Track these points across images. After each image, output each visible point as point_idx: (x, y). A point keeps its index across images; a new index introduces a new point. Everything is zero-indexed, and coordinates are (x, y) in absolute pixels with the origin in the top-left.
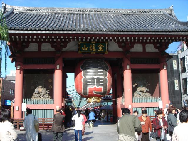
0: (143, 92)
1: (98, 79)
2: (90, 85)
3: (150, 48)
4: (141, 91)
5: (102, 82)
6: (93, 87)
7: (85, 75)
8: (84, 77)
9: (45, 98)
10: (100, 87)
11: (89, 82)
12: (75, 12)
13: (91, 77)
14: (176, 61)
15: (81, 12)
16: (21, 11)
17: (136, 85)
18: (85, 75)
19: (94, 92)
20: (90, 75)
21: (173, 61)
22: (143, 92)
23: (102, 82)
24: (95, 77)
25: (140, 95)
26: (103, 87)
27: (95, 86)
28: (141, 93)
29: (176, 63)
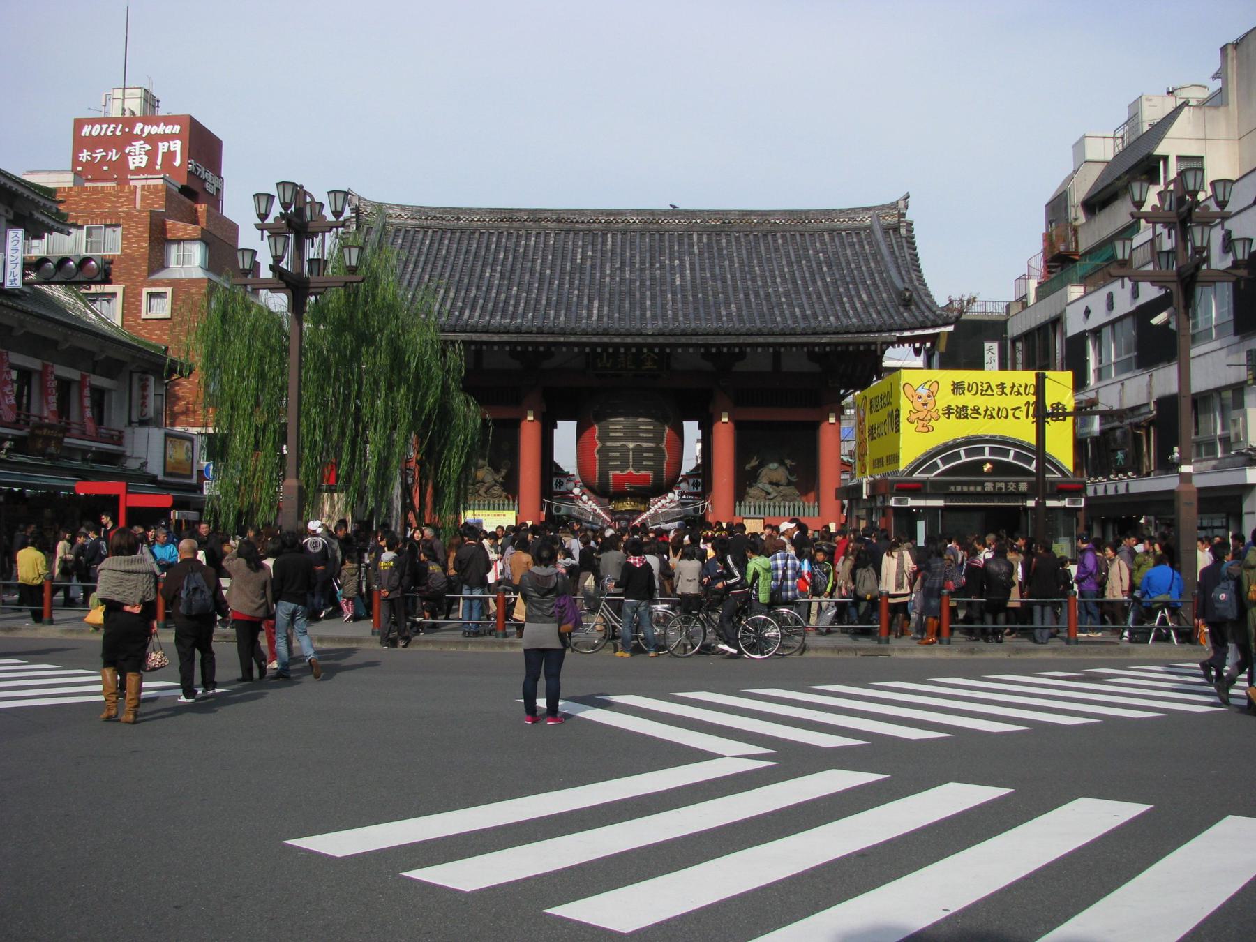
0: (777, 484)
1: (638, 450)
2: (616, 468)
3: (795, 364)
4: (771, 483)
5: (648, 459)
6: (625, 473)
7: (604, 437)
8: (599, 445)
9: (493, 496)
10: (644, 472)
11: (615, 459)
12: (580, 226)
13: (618, 444)
14: (995, 346)
15: (600, 226)
16: (409, 221)
17: (754, 463)
18: (604, 437)
19: (627, 485)
20: (616, 439)
21: (987, 345)
22: (777, 484)
23: (648, 459)
24: (631, 445)
25: (768, 494)
26: (651, 473)
27: (631, 470)
28: (769, 488)
29: (996, 357)
